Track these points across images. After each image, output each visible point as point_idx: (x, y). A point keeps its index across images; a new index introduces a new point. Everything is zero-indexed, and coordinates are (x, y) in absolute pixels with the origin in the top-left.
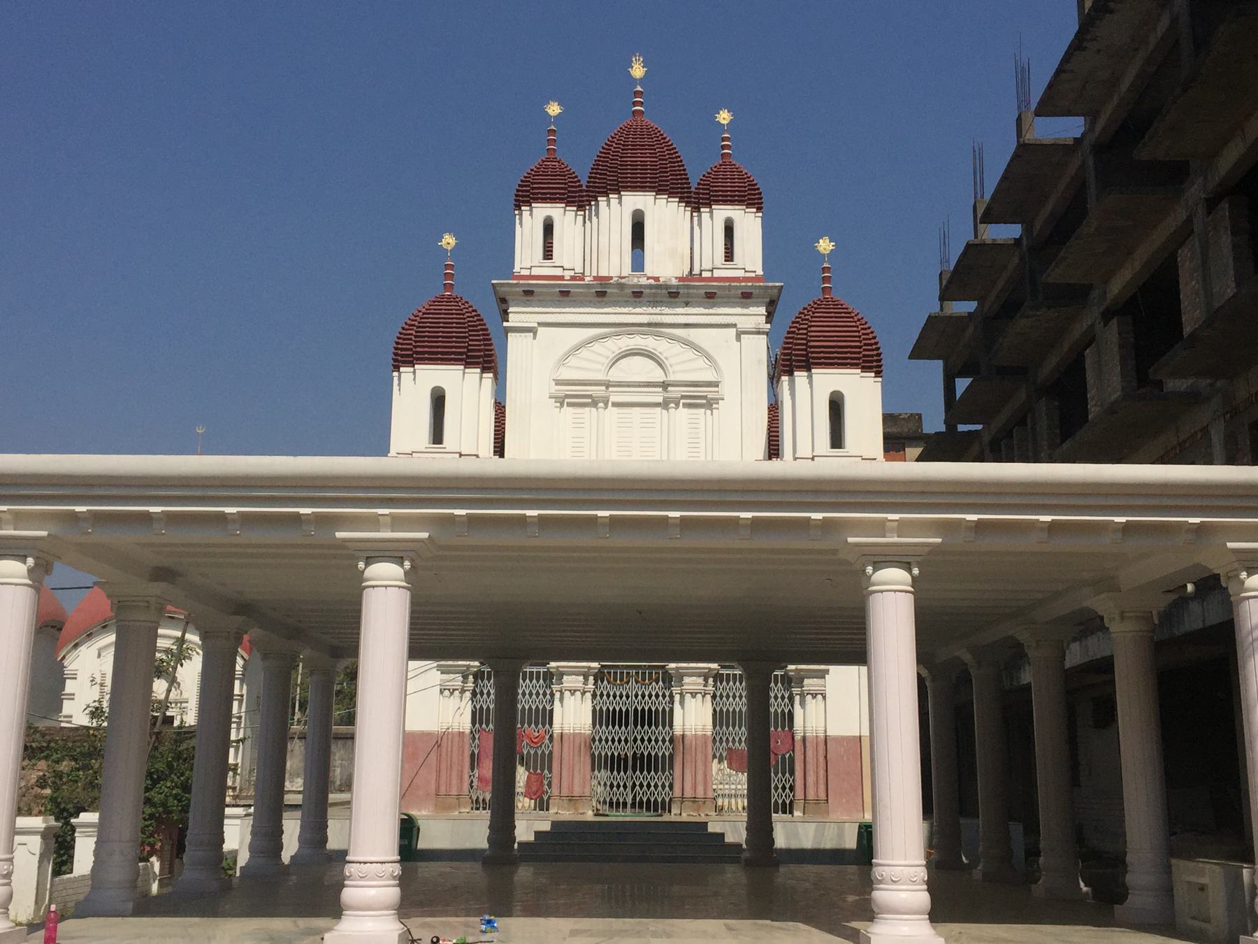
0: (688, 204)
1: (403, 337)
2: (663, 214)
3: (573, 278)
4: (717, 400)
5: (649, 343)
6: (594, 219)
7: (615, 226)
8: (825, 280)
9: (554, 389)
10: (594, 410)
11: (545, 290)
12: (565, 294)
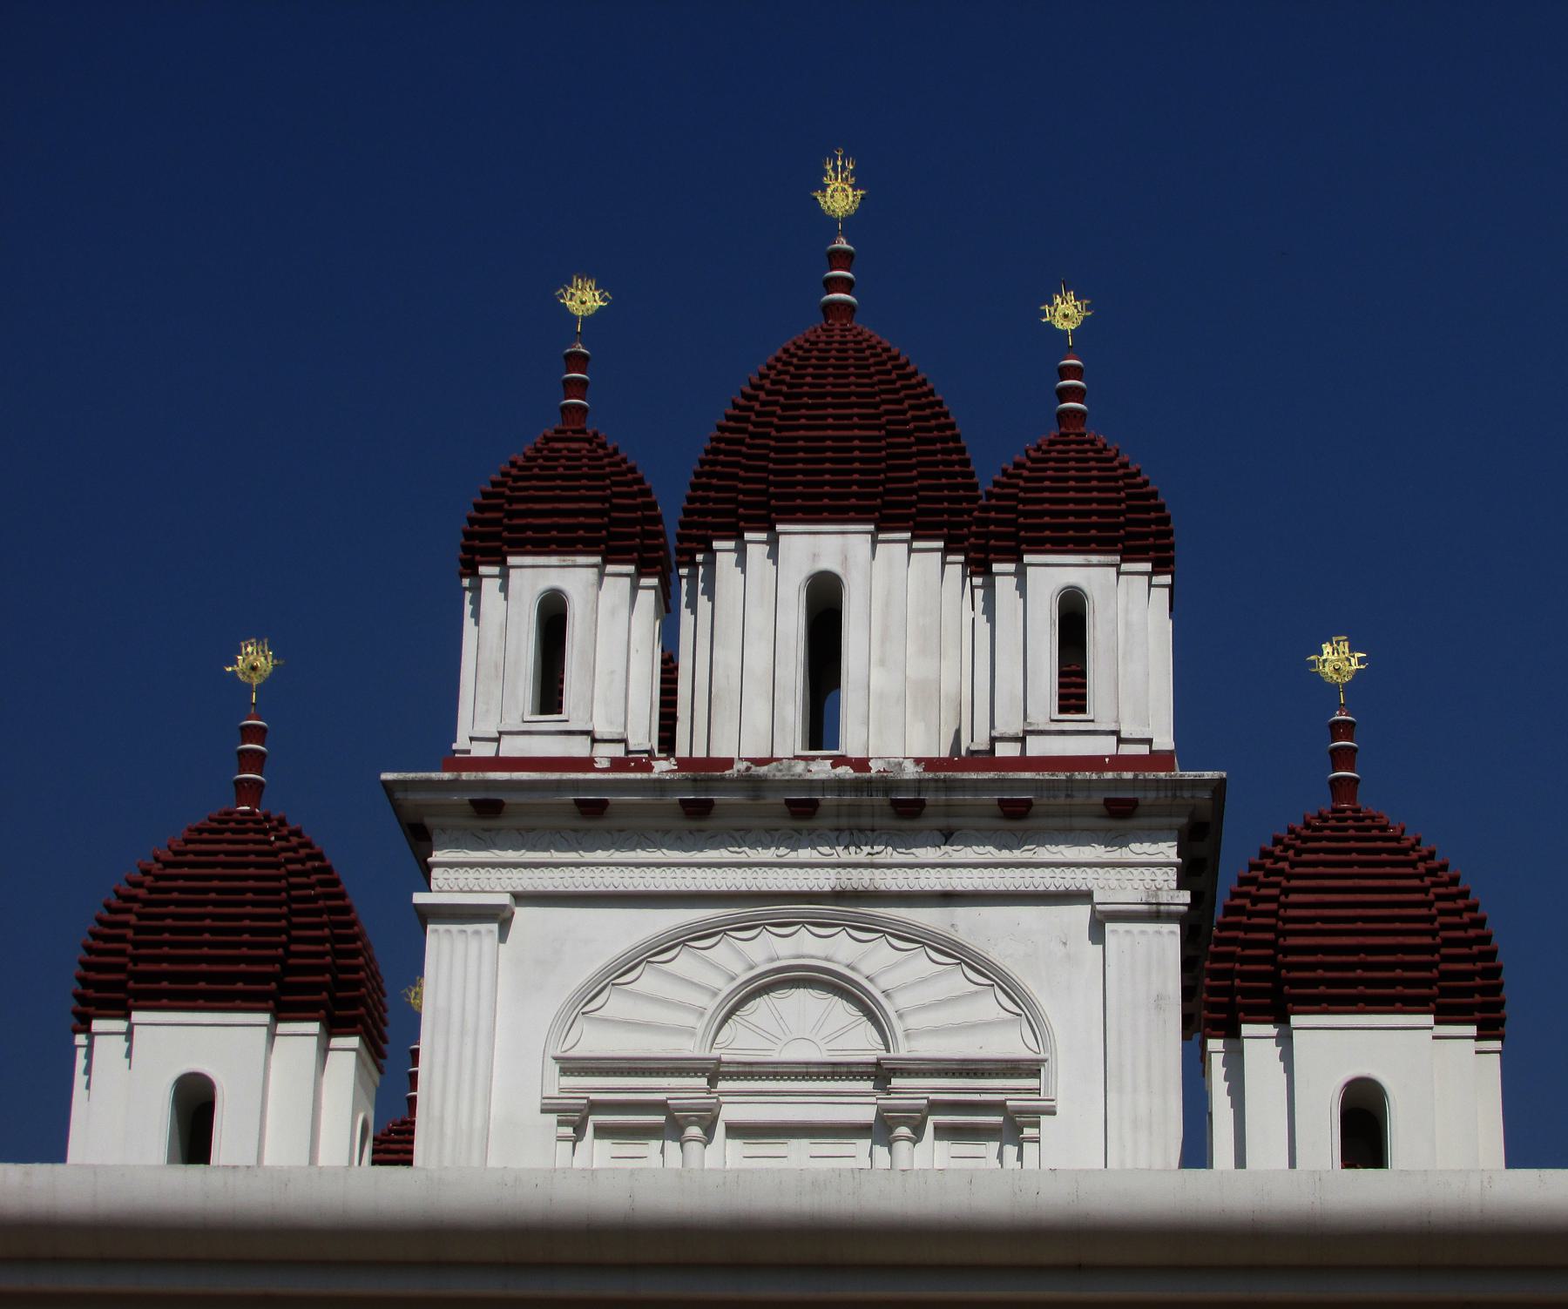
1: (106, 933)
2: (898, 587)
3: (617, 764)
4: (1034, 1116)
5: (837, 949)
6: (702, 600)
7: (759, 619)
8: (1341, 758)
9: (559, 1085)
10: (672, 1147)
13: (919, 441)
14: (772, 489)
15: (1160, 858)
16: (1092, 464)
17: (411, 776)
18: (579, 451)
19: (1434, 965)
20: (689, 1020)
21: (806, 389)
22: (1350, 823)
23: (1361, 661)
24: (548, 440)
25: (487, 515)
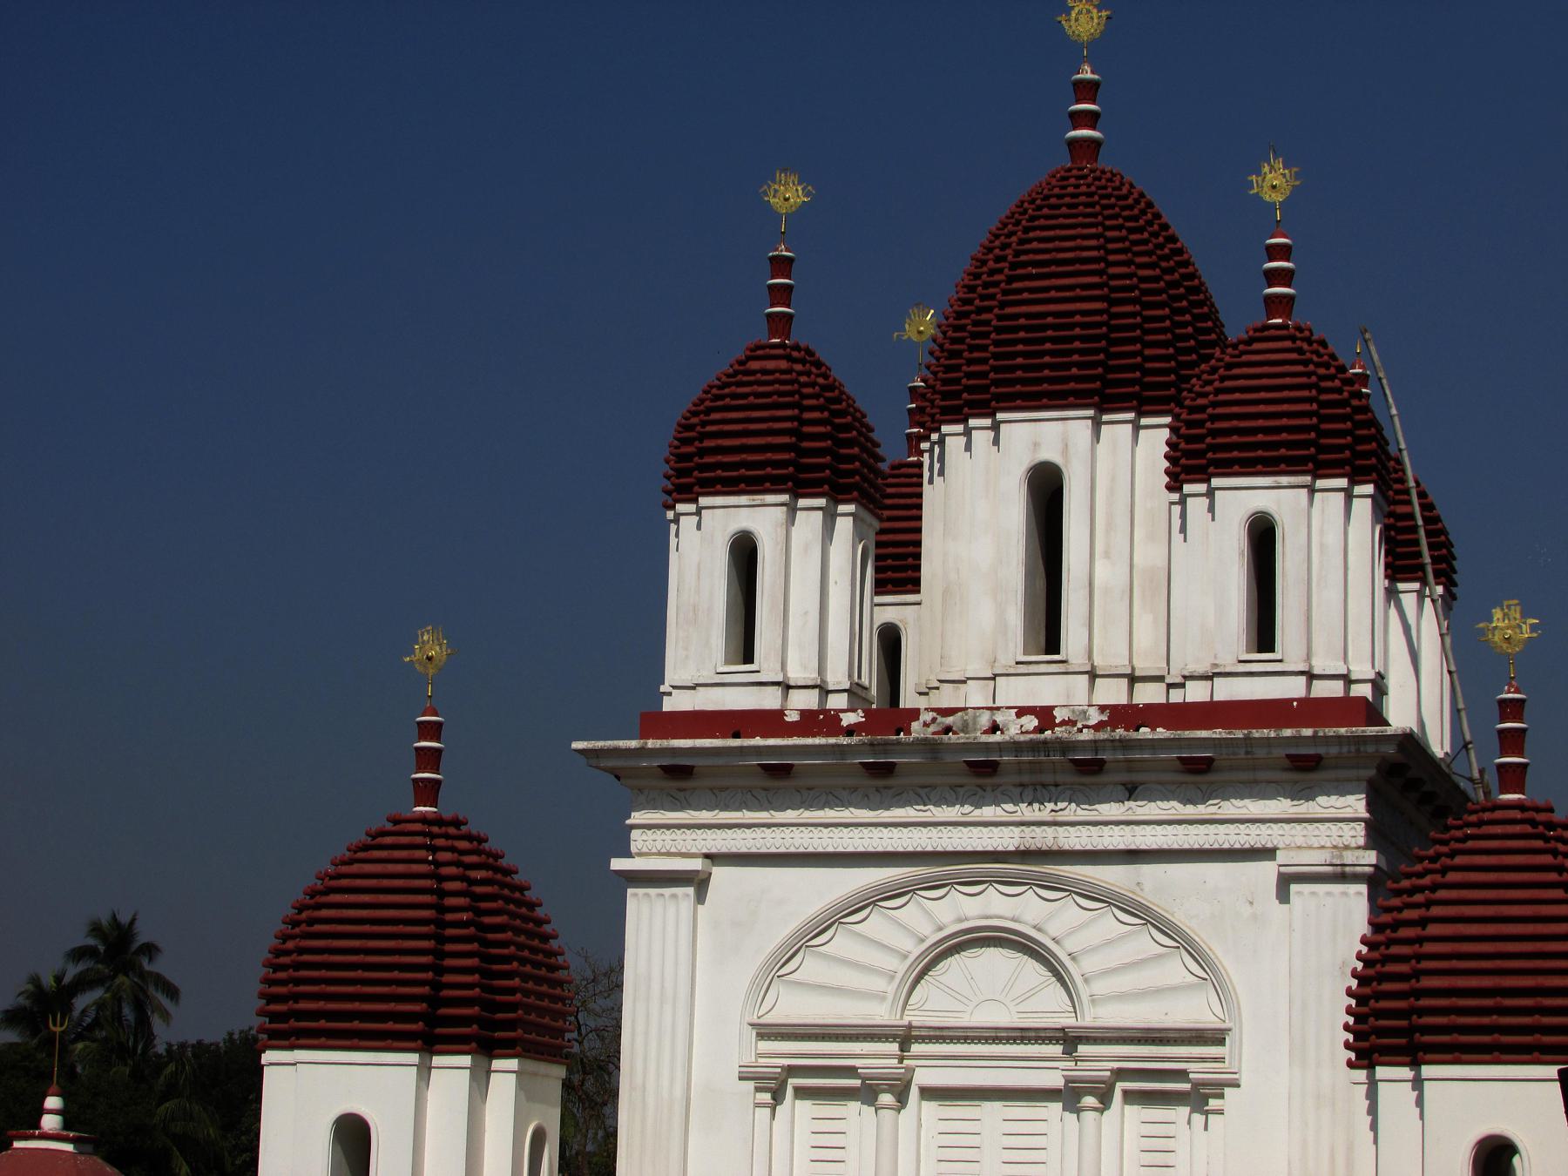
4: (1217, 1088)
15: (1348, 813)
17: (600, 744)
20: (879, 984)
23: (1533, 628)
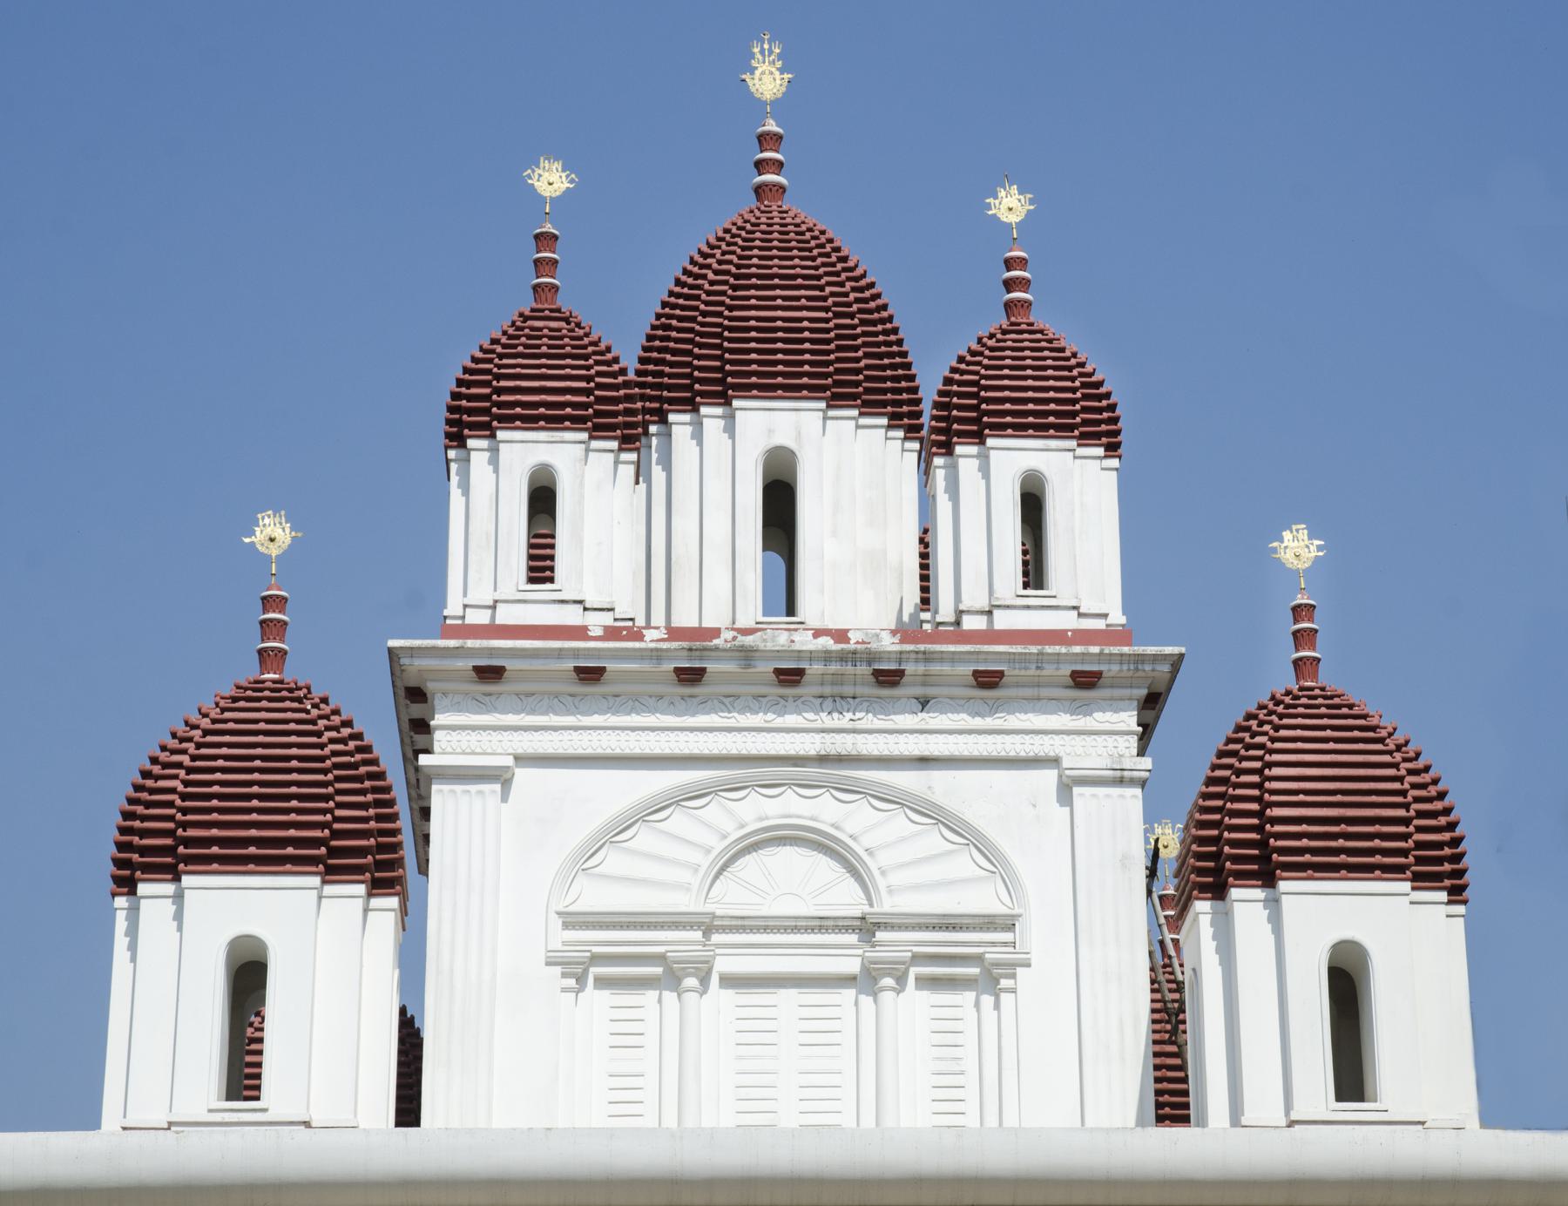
0: (912, 431)
2: (851, 463)
3: (611, 633)
4: (1010, 968)
5: (820, 809)
6: (658, 473)
7: (717, 490)
9: (560, 938)
10: (669, 997)
11: (537, 665)
12: (590, 675)
13: (863, 322)
14: (728, 367)
16: (1046, 353)
18: (559, 330)
19: (1409, 835)
20: (685, 876)
21: (754, 270)
22: (1320, 701)
23: (1319, 548)
24: (526, 318)
25: (474, 391)
